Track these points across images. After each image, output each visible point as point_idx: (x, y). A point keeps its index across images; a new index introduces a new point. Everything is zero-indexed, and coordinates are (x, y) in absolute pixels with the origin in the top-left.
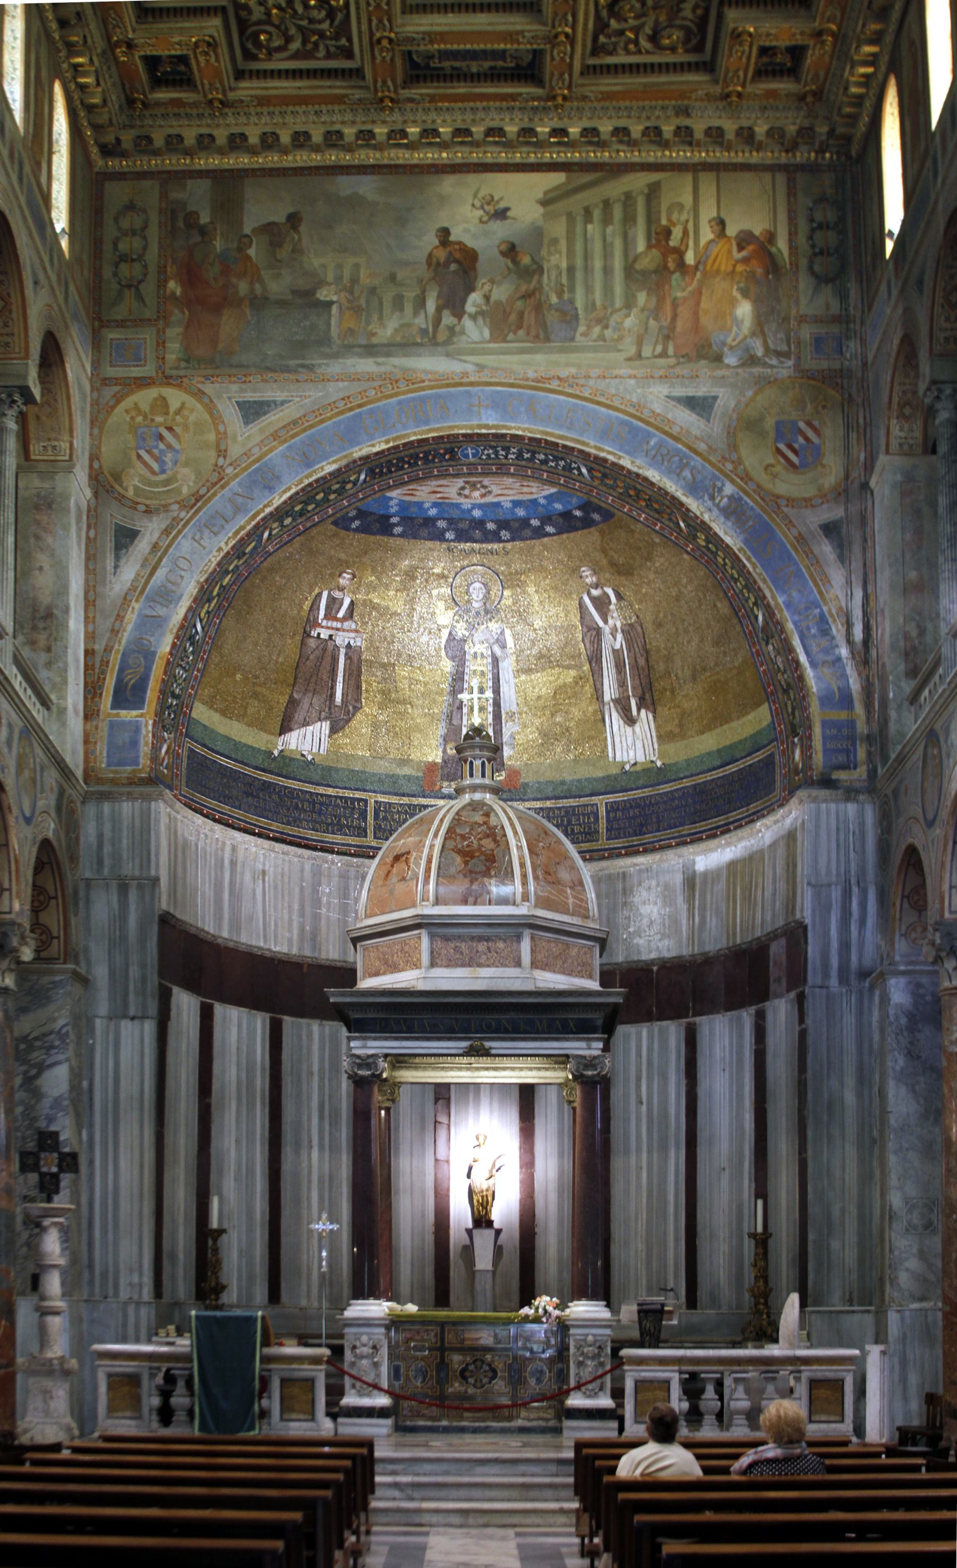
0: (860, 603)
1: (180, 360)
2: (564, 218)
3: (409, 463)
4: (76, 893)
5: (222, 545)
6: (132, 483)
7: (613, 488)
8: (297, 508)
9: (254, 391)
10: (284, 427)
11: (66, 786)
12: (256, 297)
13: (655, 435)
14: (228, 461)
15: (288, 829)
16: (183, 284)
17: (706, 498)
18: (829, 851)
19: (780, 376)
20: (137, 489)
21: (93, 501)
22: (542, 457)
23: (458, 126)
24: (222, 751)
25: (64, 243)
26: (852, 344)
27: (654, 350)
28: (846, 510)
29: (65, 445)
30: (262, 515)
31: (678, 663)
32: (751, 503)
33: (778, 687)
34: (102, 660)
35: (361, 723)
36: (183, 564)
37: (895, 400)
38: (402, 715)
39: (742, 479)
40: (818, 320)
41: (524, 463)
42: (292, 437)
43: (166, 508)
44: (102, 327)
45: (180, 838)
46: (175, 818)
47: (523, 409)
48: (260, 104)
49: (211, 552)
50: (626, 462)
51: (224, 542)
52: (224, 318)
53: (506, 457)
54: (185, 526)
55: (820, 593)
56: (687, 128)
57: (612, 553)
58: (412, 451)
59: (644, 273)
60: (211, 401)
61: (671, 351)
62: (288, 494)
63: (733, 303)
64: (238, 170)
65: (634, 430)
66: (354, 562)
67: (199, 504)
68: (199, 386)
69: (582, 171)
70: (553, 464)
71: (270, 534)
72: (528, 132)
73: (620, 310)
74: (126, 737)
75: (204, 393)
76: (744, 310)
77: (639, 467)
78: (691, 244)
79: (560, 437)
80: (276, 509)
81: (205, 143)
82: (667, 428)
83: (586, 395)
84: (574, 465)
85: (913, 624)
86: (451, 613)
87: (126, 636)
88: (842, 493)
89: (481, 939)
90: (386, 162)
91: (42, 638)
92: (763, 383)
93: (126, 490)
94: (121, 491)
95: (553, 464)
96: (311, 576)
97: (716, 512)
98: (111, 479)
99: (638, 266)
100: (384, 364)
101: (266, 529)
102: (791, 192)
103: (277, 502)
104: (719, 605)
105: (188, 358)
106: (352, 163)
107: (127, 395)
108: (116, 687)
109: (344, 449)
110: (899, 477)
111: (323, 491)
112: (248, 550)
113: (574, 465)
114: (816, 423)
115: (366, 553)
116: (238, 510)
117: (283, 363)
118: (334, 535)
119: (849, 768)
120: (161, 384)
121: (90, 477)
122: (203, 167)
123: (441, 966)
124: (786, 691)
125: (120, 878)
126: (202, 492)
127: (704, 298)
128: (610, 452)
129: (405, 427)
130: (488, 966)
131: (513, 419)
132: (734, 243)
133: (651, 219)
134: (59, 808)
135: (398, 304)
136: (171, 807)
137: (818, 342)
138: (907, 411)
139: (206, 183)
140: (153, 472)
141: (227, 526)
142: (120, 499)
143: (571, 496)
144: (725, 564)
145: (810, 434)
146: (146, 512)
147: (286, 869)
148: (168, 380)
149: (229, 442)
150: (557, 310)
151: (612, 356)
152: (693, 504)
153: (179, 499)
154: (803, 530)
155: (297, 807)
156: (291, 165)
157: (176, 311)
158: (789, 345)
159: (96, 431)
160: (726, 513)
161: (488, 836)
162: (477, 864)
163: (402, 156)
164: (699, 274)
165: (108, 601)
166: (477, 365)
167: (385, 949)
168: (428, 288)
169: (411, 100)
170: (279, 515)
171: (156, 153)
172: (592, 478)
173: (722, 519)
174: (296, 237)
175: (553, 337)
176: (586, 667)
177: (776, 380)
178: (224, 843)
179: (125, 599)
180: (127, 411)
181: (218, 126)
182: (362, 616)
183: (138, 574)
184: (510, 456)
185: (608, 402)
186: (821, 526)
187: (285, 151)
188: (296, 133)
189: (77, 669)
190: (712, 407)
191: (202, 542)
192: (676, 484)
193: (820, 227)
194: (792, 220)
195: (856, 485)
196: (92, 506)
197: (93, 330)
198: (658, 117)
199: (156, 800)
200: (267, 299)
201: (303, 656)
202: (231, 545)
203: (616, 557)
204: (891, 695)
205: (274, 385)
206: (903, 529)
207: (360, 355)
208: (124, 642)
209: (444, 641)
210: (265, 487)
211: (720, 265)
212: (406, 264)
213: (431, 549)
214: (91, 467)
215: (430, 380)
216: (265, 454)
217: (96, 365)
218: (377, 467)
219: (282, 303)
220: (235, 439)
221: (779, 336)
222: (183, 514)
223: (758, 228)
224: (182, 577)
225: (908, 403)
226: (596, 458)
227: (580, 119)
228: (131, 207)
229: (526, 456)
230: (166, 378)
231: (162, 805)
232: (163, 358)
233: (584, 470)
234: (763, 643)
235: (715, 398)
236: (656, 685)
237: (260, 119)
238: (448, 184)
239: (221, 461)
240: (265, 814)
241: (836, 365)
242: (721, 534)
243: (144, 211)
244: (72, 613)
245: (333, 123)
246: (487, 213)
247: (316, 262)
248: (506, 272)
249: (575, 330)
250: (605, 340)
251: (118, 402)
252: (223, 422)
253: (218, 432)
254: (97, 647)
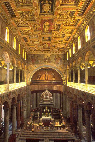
6: (29, 70)
51: (34, 73)
76: (60, 61)
105: (32, 64)
133: (55, 57)
135: (43, 61)
148: (31, 65)
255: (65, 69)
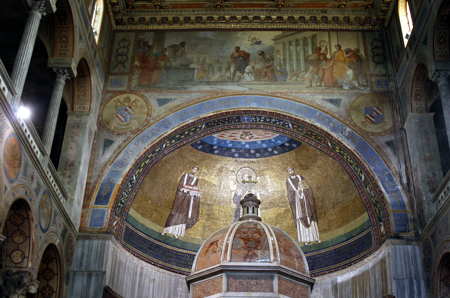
0: (404, 170)
1: (137, 85)
2: (282, 44)
3: (222, 122)
4: (68, 276)
5: (146, 146)
6: (114, 125)
7: (302, 132)
8: (177, 136)
9: (164, 95)
10: (174, 107)
11: (68, 228)
12: (167, 66)
13: (318, 112)
14: (151, 118)
15: (166, 264)
16: (140, 62)
17: (339, 133)
18: (402, 266)
19: (365, 93)
20: (115, 127)
21: (97, 130)
22: (274, 120)
23: (243, 16)
24: (140, 230)
25: (97, 38)
26: (391, 83)
27: (316, 84)
28: (395, 137)
29: (88, 106)
30: (163, 137)
31: (327, 202)
32: (357, 135)
33: (372, 204)
34: (93, 186)
35: (198, 226)
36: (130, 153)
37: (414, 93)
38: (215, 224)
39: (353, 126)
40: (377, 75)
41: (266, 123)
42: (177, 110)
43: (125, 133)
44: (109, 75)
45: (118, 259)
46: (117, 251)
47: (267, 103)
48: (173, 8)
49: (142, 149)
50: (307, 120)
51: (147, 146)
52: (155, 73)
53: (260, 121)
54: (132, 140)
55: (388, 166)
56: (326, 17)
57: (300, 161)
58: (223, 117)
59: (312, 61)
60: (147, 98)
61: (323, 85)
62: (174, 130)
63: (346, 70)
64: (164, 30)
65: (310, 110)
66: (199, 163)
67: (138, 132)
68: (143, 94)
69: (288, 31)
70: (278, 123)
71: (166, 146)
72: (268, 18)
73: (303, 72)
74: (99, 215)
75: (144, 96)
76: (350, 72)
77: (312, 122)
78: (329, 52)
79: (281, 112)
80: (169, 135)
81: (153, 21)
82: (323, 109)
83: (291, 98)
84: (286, 123)
85: (430, 172)
86: (236, 186)
87: (103, 178)
88: (393, 131)
89: (253, 278)
90: (217, 28)
91: (68, 173)
92: (359, 95)
93: (111, 127)
94: (109, 127)
95: (278, 123)
96: (182, 167)
97: (343, 137)
98: (105, 123)
99: (309, 59)
100: (214, 87)
101: (164, 143)
102: (364, 37)
103: (169, 132)
104: (344, 177)
106: (205, 28)
107: (115, 96)
108: (97, 196)
109: (197, 115)
110: (417, 121)
111: (188, 131)
112: (157, 150)
113: (286, 123)
114: (380, 108)
115: (204, 160)
116: (153, 134)
117: (176, 87)
118: (191, 151)
119: (407, 232)
120: (128, 93)
121: (97, 123)
122: (152, 29)
123: (232, 291)
124: (375, 205)
125: (89, 271)
126: (140, 128)
127: (334, 69)
128: (301, 117)
129: (221, 108)
130: (256, 292)
131: (263, 106)
132: (345, 52)
133: (313, 45)
134: (63, 235)
136: (116, 245)
137: (378, 82)
138: (418, 97)
139: (152, 34)
140: (122, 121)
141: (149, 140)
142: (108, 130)
143: (284, 137)
144: (347, 158)
145: (378, 111)
146: (117, 134)
147: (164, 279)
148: (131, 92)
149: (152, 112)
150: (279, 72)
151: (300, 86)
152: (334, 135)
153: (131, 131)
154: (379, 144)
155: (170, 256)
156: (183, 28)
157: (137, 71)
158: (367, 83)
159: (102, 108)
160: (348, 138)
161: (257, 232)
162: (251, 244)
163: (223, 26)
164: (332, 61)
165: (98, 165)
166: (249, 88)
167: (204, 285)
168: (231, 64)
169: (227, 6)
170: (170, 137)
171: (136, 24)
172: (293, 128)
173: (346, 140)
174: (183, 49)
175: (278, 80)
176: (289, 206)
177: (363, 94)
178: (138, 265)
179: (105, 164)
180: (115, 101)
181: (158, 15)
182: (201, 185)
183: (111, 156)
184: (261, 121)
185: (300, 101)
186: (386, 143)
187: (181, 24)
188: (185, 17)
189: (82, 187)
190: (340, 102)
191: (138, 145)
192: (327, 128)
193: (376, 47)
194: (365, 45)
195: (398, 128)
196: (97, 132)
197: (106, 76)
198: (315, 14)
199: (108, 240)
200: (171, 67)
201: (176, 198)
202: (150, 146)
203: (302, 162)
204: (424, 199)
205: (172, 94)
206: (422, 138)
207: (205, 85)
208: (103, 180)
209: (232, 196)
210: (165, 127)
211: (340, 58)
212: (223, 57)
213: (229, 161)
214: (98, 119)
215: (231, 93)
216: (166, 116)
217: (105, 86)
218: (209, 123)
219: (176, 68)
220: (155, 111)
221: (363, 80)
222: (132, 136)
223: (353, 47)
224: (129, 157)
225: (419, 95)
226: (295, 119)
227: (287, 14)
228: (124, 40)
229: (268, 120)
230: (131, 91)
231: (111, 243)
232: (130, 85)
233: (290, 125)
234: (364, 187)
235: (341, 100)
236: (318, 212)
237: (173, 13)
238: (239, 34)
239: (149, 118)
240: (157, 257)
241: (386, 89)
242: (346, 145)
243: (129, 41)
244: (82, 164)
245: (199, 14)
246: (254, 43)
247: (190, 56)
248: (260, 60)
249: (286, 78)
250: (298, 81)
251: (112, 98)
252: (151, 105)
253: (148, 108)
254: (91, 181)
255: (398, 125)
